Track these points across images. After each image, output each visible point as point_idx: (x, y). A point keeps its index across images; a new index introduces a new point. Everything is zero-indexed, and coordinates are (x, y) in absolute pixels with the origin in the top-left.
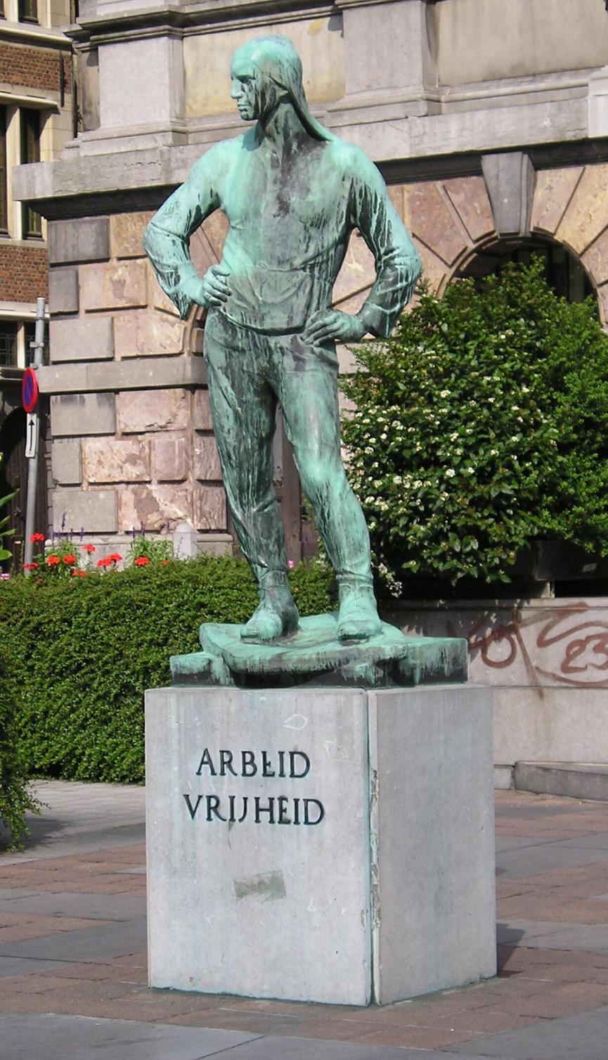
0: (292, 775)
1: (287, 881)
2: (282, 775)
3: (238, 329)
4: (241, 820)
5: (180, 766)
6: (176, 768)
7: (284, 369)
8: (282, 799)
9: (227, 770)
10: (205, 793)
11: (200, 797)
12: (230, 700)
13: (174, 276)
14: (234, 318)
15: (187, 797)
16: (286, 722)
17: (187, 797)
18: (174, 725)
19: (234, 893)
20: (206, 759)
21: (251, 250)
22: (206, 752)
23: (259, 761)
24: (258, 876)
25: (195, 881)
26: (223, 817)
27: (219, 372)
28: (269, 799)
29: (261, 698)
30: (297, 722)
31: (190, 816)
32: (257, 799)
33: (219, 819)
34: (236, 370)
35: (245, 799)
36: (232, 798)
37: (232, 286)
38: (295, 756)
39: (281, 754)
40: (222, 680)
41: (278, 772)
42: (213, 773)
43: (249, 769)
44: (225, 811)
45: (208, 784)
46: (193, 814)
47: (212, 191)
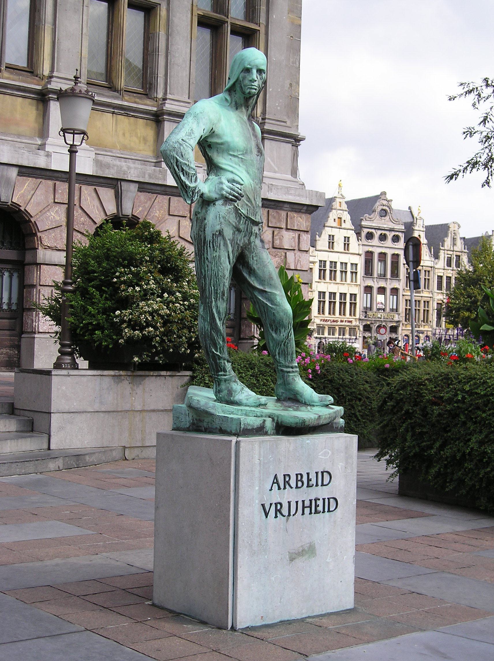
0: (322, 485)
1: (317, 546)
2: (317, 485)
3: (242, 218)
4: (293, 515)
5: (260, 487)
6: (257, 488)
7: (256, 246)
8: (316, 500)
9: (287, 486)
10: (274, 502)
11: (271, 504)
12: (290, 444)
13: (195, 177)
14: (244, 211)
15: (263, 505)
16: (320, 454)
17: (263, 505)
18: (257, 461)
19: (288, 559)
20: (275, 481)
21: (251, 173)
22: (276, 477)
23: (305, 479)
24: (302, 546)
25: (266, 557)
26: (284, 514)
27: (228, 242)
28: (310, 500)
29: (307, 442)
30: (325, 454)
31: (265, 517)
32: (303, 501)
33: (281, 516)
34: (235, 242)
35: (297, 502)
36: (289, 503)
37: (244, 191)
38: (325, 473)
39: (317, 473)
40: (269, 432)
41: (315, 484)
42: (279, 488)
43: (300, 484)
44: (285, 511)
45: (276, 496)
46: (267, 515)
47: (213, 128)
